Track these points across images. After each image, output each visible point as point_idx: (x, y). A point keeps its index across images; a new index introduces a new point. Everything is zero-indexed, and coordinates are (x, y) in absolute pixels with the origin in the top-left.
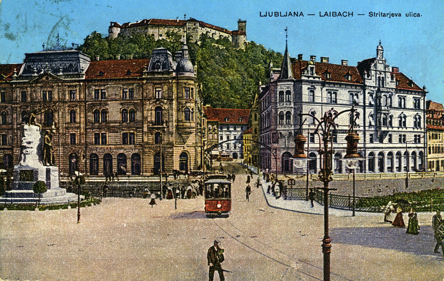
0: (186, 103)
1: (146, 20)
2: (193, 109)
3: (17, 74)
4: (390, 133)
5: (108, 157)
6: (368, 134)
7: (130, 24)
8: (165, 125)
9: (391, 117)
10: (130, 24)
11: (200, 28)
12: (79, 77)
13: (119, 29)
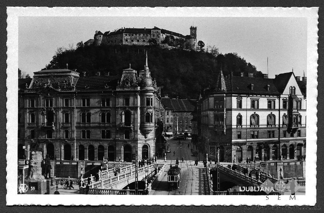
0: (147, 109)
1: (122, 29)
2: (152, 114)
3: (28, 87)
4: (299, 129)
5: (91, 148)
6: (281, 131)
7: (110, 33)
8: (132, 125)
9: (301, 117)
10: (110, 33)
11: (162, 34)
12: (71, 90)
13: (102, 36)
